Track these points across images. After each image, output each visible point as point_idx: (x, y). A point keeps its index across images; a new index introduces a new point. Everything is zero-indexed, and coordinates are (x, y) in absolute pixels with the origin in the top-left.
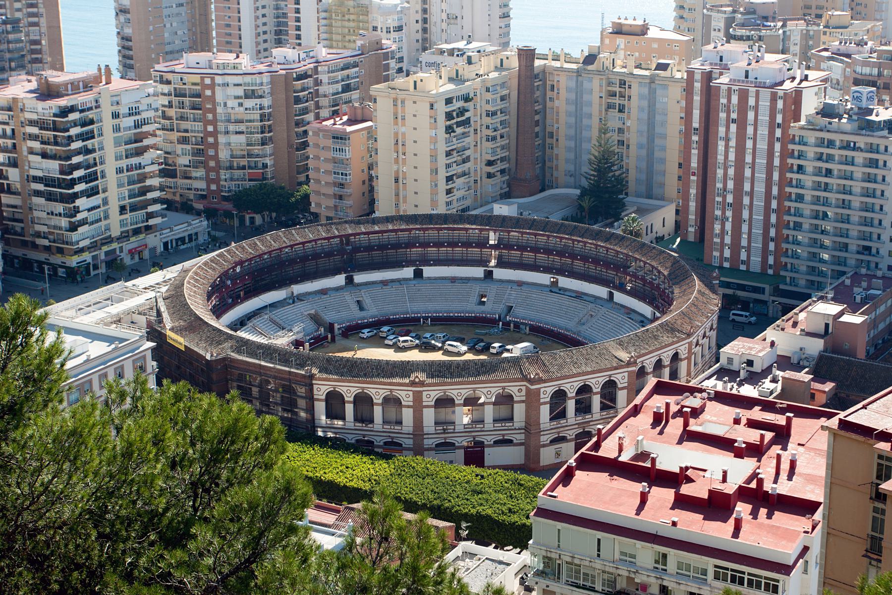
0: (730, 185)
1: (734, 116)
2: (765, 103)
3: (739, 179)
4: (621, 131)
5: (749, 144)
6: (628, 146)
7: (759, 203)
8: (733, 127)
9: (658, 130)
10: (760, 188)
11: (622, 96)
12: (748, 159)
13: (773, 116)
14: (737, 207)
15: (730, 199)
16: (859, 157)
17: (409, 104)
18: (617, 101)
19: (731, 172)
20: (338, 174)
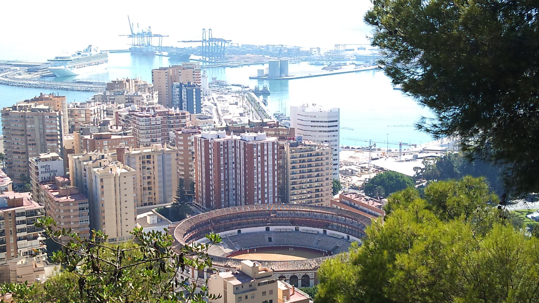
0: (260, 180)
1: (259, 154)
2: (270, 147)
3: (263, 177)
4: (149, 177)
5: (266, 163)
6: (154, 183)
7: (271, 185)
8: (259, 158)
9: (167, 173)
10: (271, 179)
11: (148, 162)
12: (266, 169)
13: (273, 151)
14: (263, 187)
15: (260, 186)
16: (314, 158)
17: (122, 178)
18: (147, 165)
19: (260, 175)
20: (83, 221)
